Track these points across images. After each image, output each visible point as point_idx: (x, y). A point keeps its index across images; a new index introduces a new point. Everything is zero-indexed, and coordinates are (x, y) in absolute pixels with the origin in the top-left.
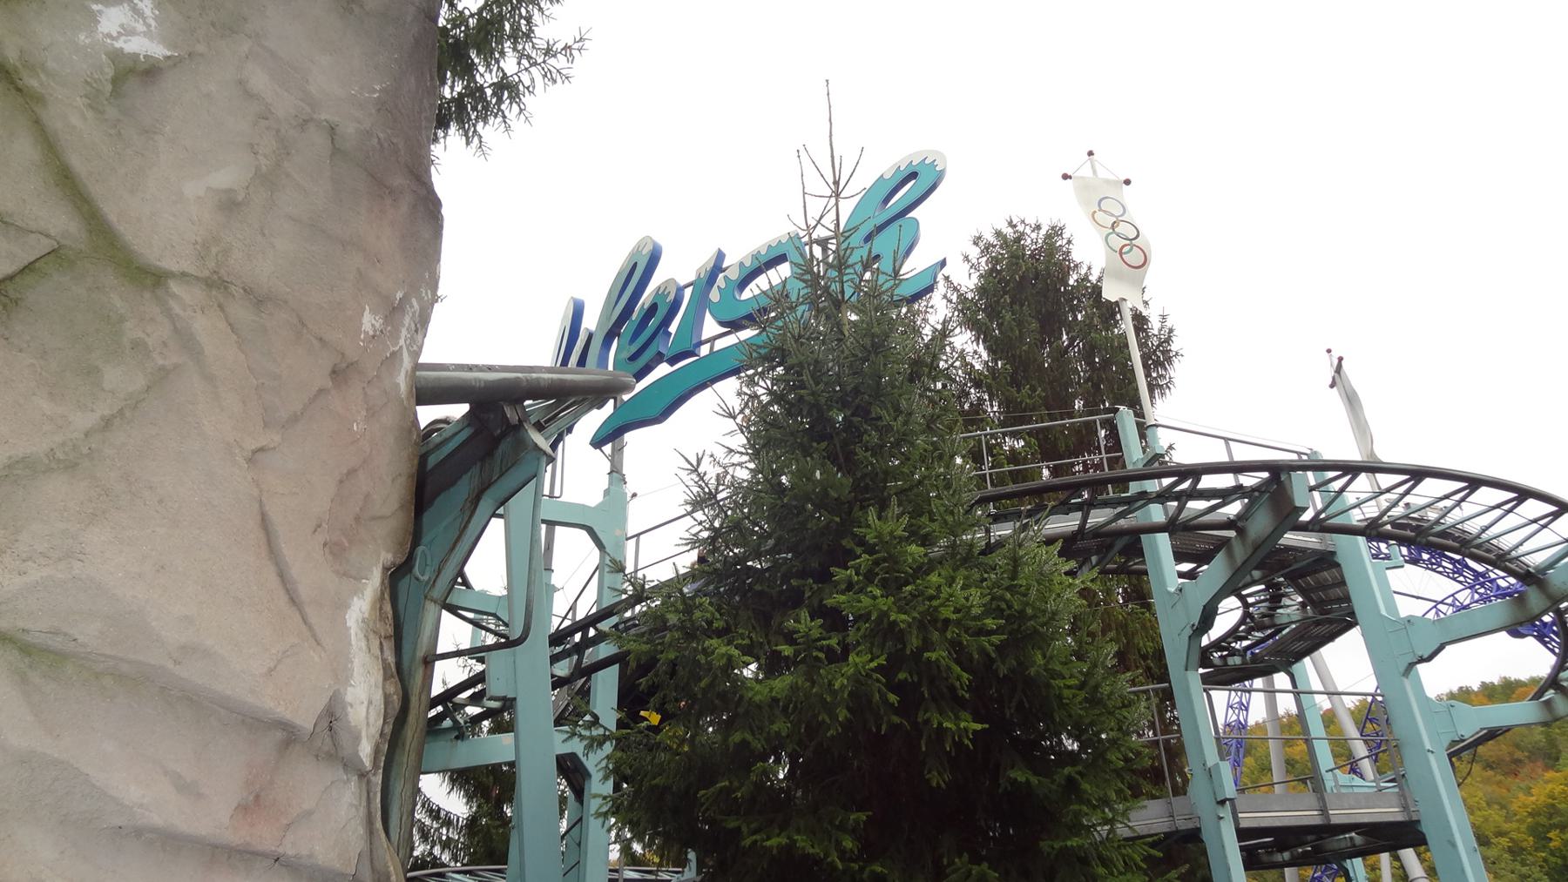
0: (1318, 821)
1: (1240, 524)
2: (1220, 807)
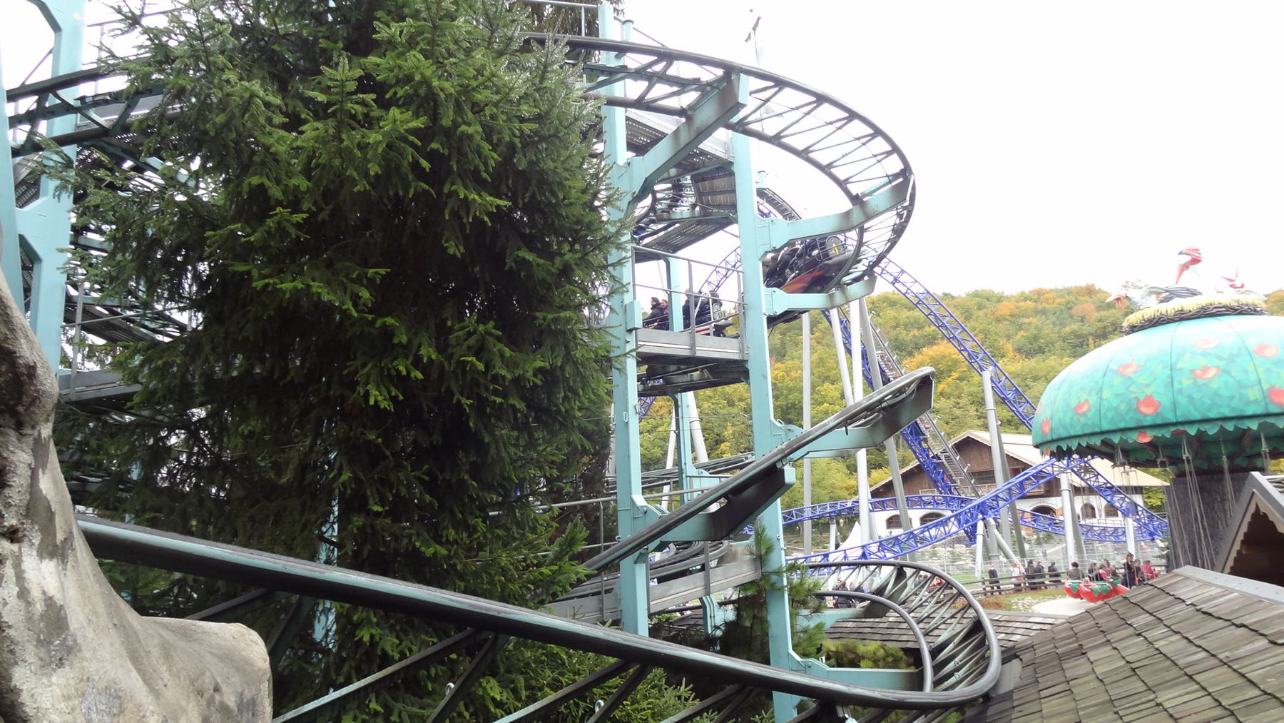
0: (686, 353)
1: (689, 113)
2: (628, 334)
